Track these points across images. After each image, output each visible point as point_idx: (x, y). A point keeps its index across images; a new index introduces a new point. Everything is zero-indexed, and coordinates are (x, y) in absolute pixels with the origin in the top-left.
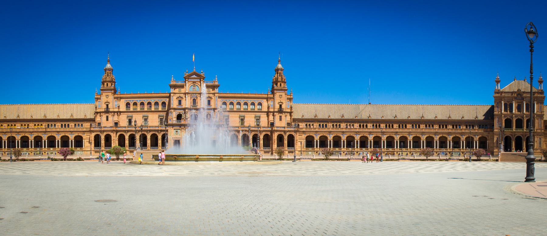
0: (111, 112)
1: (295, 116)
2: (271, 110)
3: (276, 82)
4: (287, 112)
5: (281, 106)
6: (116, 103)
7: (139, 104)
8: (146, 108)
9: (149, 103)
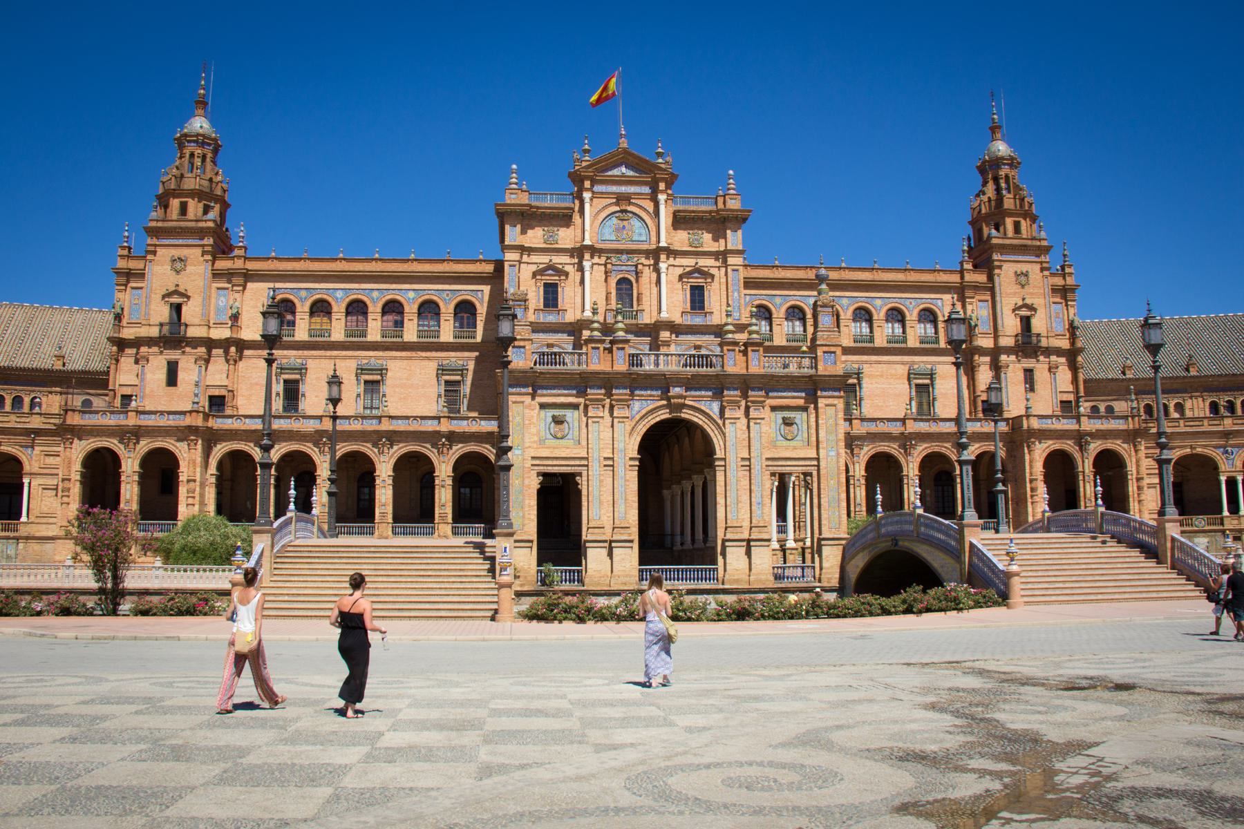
0: (195, 342)
1: (1091, 368)
2: (986, 342)
3: (996, 216)
4: (1059, 352)
5: (1026, 322)
6: (222, 302)
7: (339, 309)
8: (375, 329)
9: (393, 308)
